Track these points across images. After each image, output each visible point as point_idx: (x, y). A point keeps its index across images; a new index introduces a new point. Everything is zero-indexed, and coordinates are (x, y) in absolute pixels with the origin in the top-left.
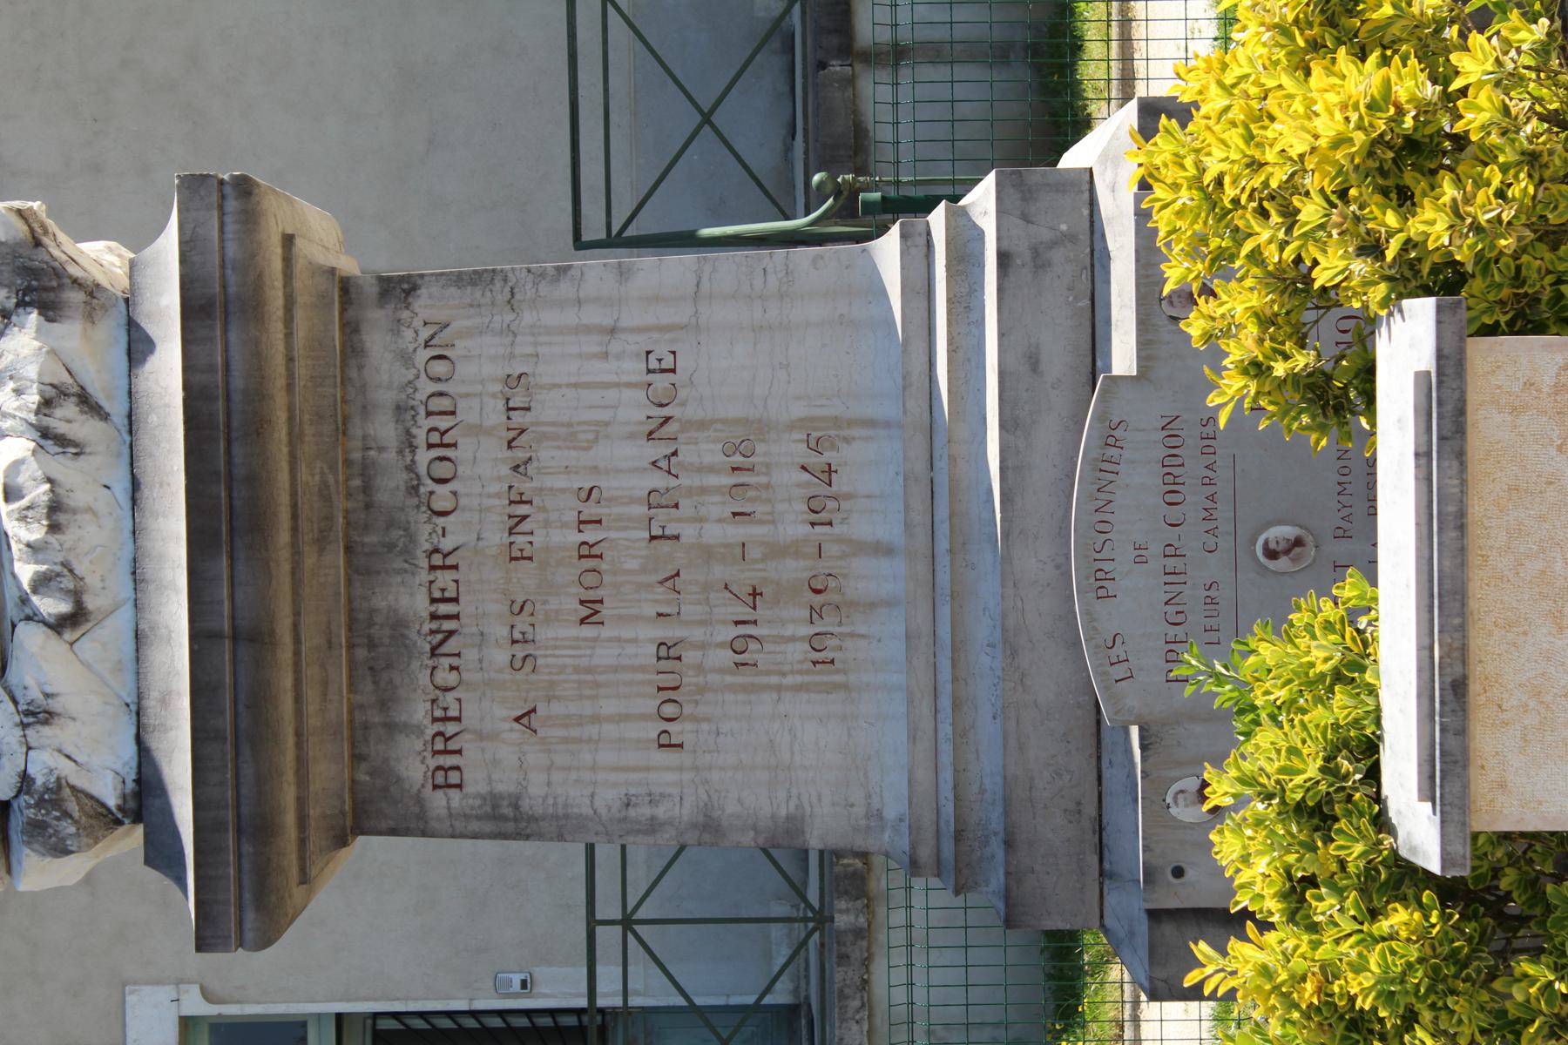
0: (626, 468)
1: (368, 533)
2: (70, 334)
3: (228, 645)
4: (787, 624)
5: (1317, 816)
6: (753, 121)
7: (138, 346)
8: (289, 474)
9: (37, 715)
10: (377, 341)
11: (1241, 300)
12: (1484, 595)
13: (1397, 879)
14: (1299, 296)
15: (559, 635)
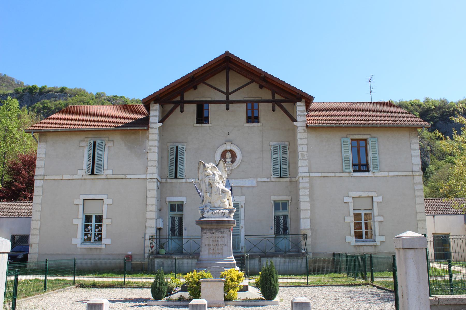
0: (220, 243)
1: (217, 229)
2: (228, 214)
3: (211, 222)
4: (212, 251)
5: (202, 276)
6: (255, 250)
7: (227, 217)
8: (220, 225)
9: (208, 212)
10: (227, 230)
11: (226, 273)
12: (212, 283)
13: (199, 279)
14: (225, 276)
15: (212, 239)
